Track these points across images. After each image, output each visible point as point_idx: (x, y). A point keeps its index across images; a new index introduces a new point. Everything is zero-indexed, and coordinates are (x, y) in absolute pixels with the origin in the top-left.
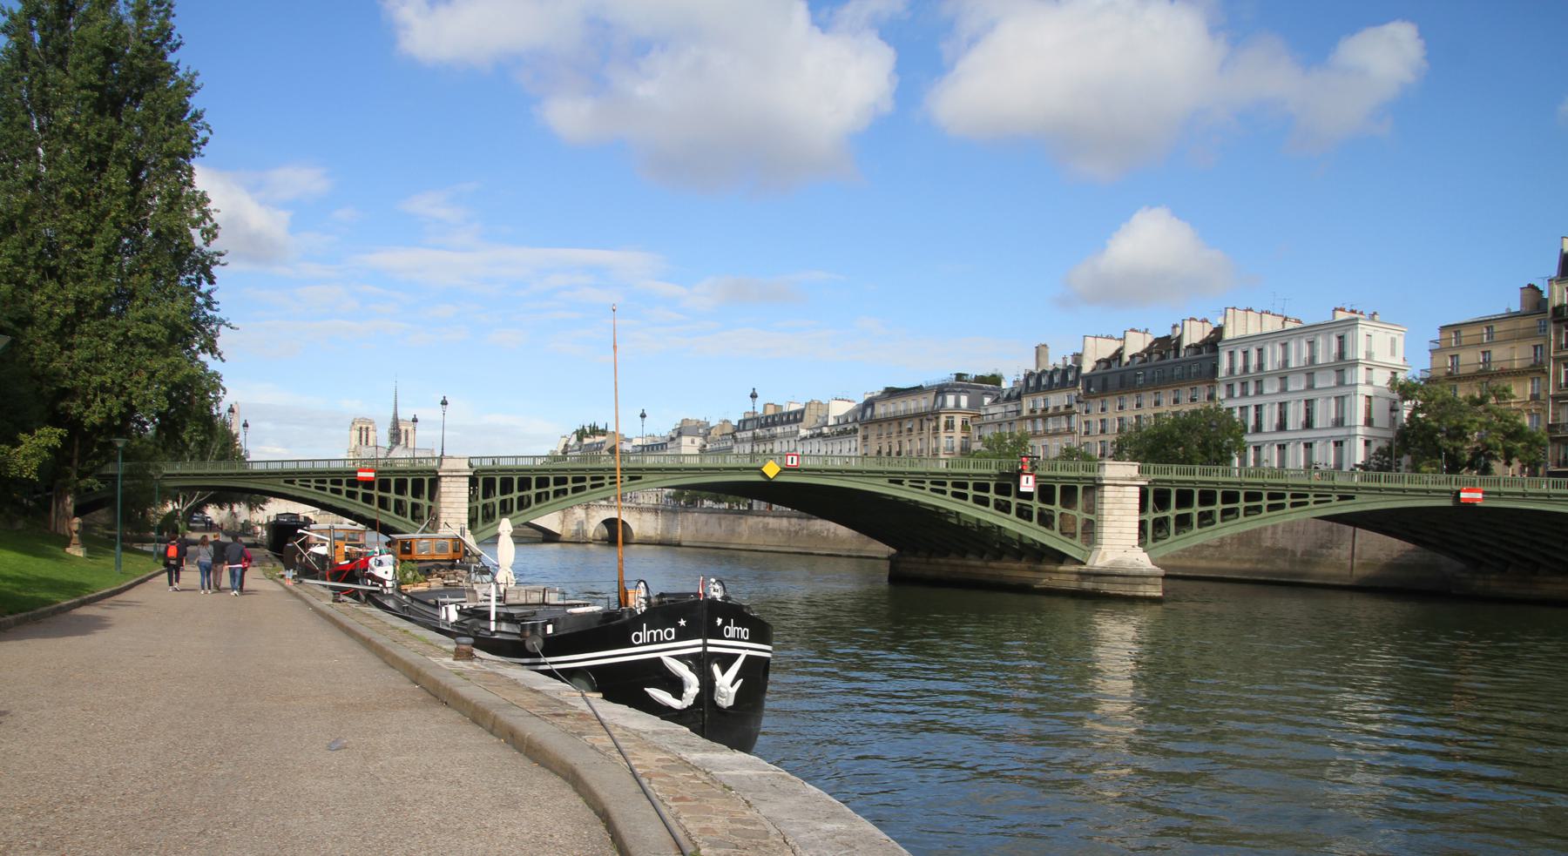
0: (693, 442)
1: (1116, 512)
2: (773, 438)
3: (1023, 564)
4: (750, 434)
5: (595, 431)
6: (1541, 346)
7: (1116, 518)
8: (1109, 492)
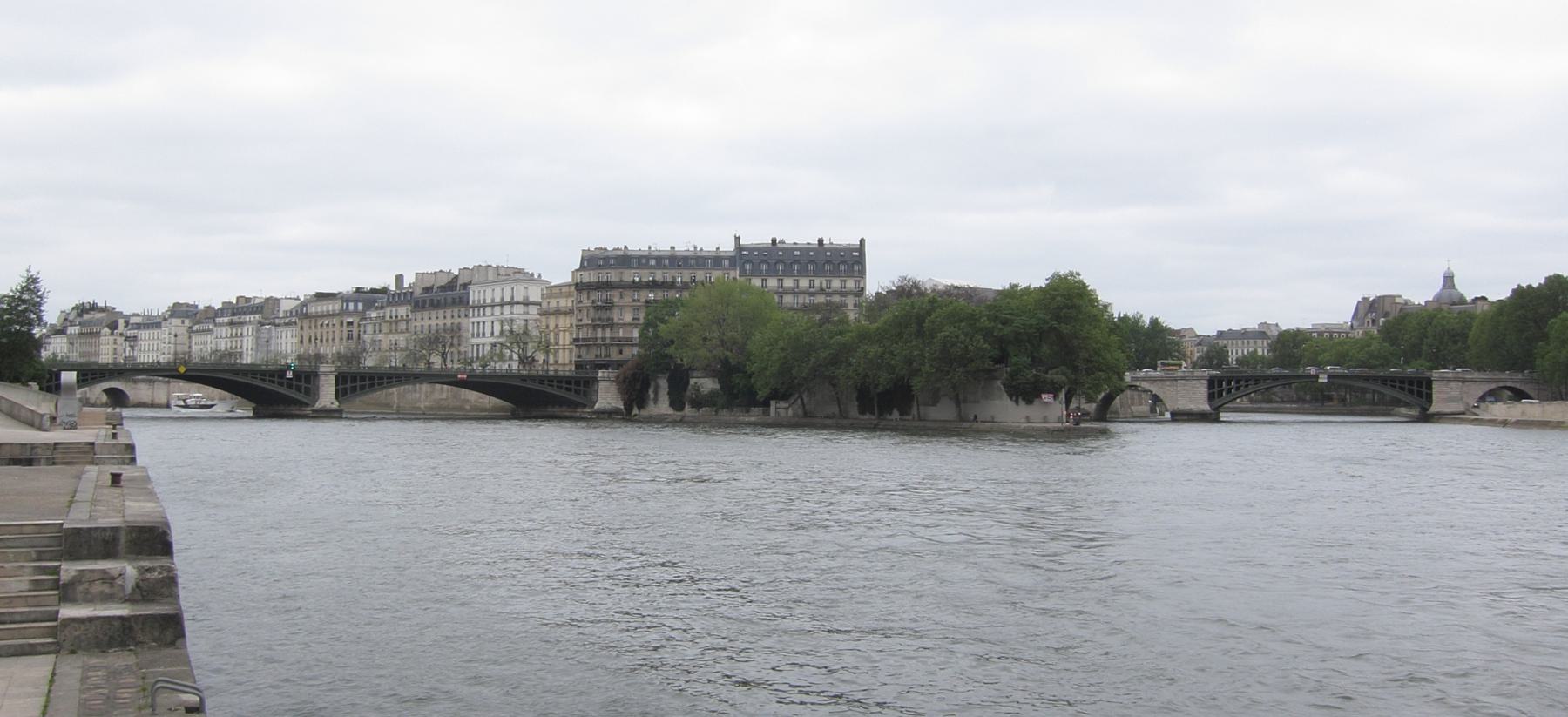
0: (183, 322)
2: (242, 324)
4: (226, 320)
5: (94, 308)
8: (323, 378)
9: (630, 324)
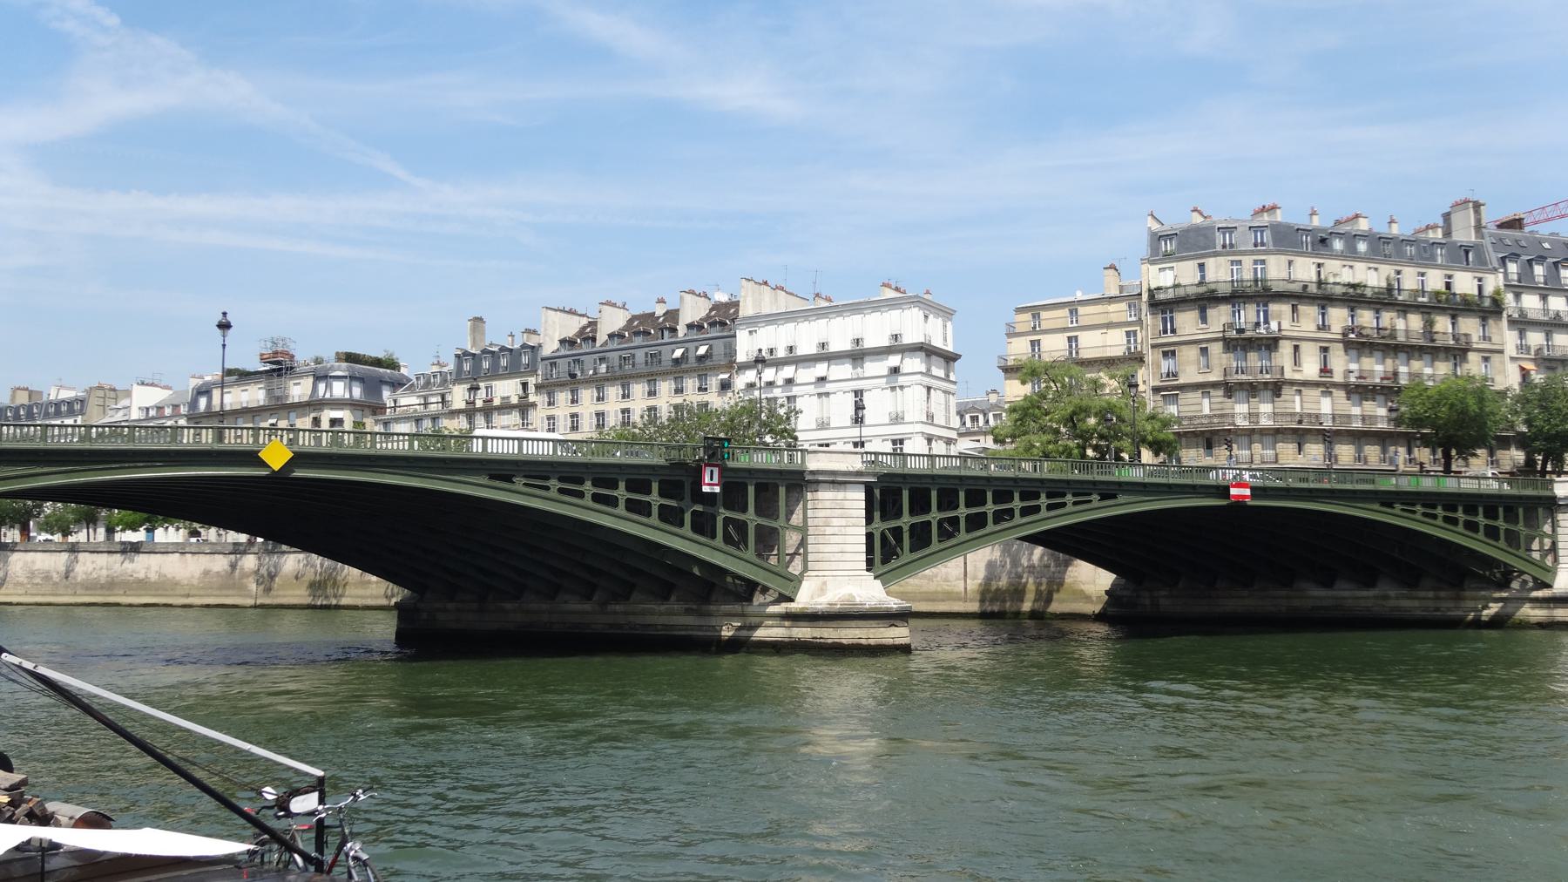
1: (835, 522)
3: (674, 605)
6: (1135, 332)
7: (836, 530)
9: (1316, 384)
